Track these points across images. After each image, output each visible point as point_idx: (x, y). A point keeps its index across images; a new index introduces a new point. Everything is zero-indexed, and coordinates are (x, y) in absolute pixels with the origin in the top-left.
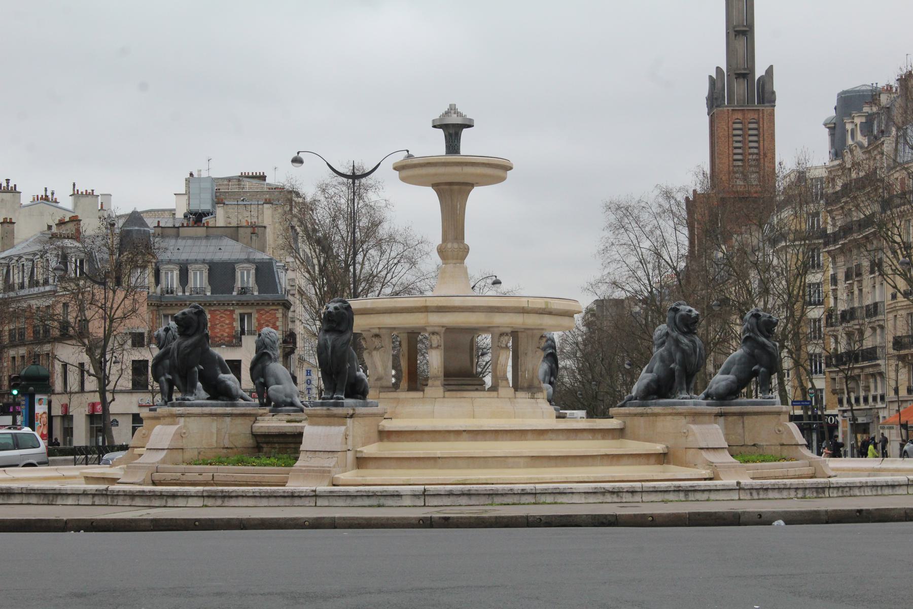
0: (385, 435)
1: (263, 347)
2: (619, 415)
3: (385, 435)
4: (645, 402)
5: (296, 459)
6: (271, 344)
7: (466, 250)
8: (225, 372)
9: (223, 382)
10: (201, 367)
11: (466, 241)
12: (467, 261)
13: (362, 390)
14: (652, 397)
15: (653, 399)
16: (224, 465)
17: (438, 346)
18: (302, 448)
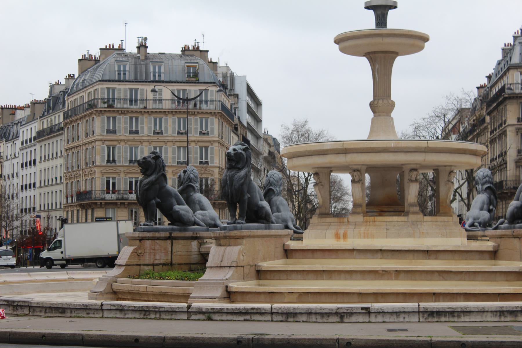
0: (288, 253)
1: (189, 180)
2: (492, 238)
3: (288, 253)
4: (513, 225)
5: (204, 272)
6: (195, 178)
7: (392, 105)
8: (179, 203)
9: (178, 212)
10: (159, 200)
11: (393, 98)
12: (393, 114)
13: (264, 216)
14: (517, 221)
15: (518, 223)
16: (141, 279)
17: (359, 180)
18: (208, 264)
